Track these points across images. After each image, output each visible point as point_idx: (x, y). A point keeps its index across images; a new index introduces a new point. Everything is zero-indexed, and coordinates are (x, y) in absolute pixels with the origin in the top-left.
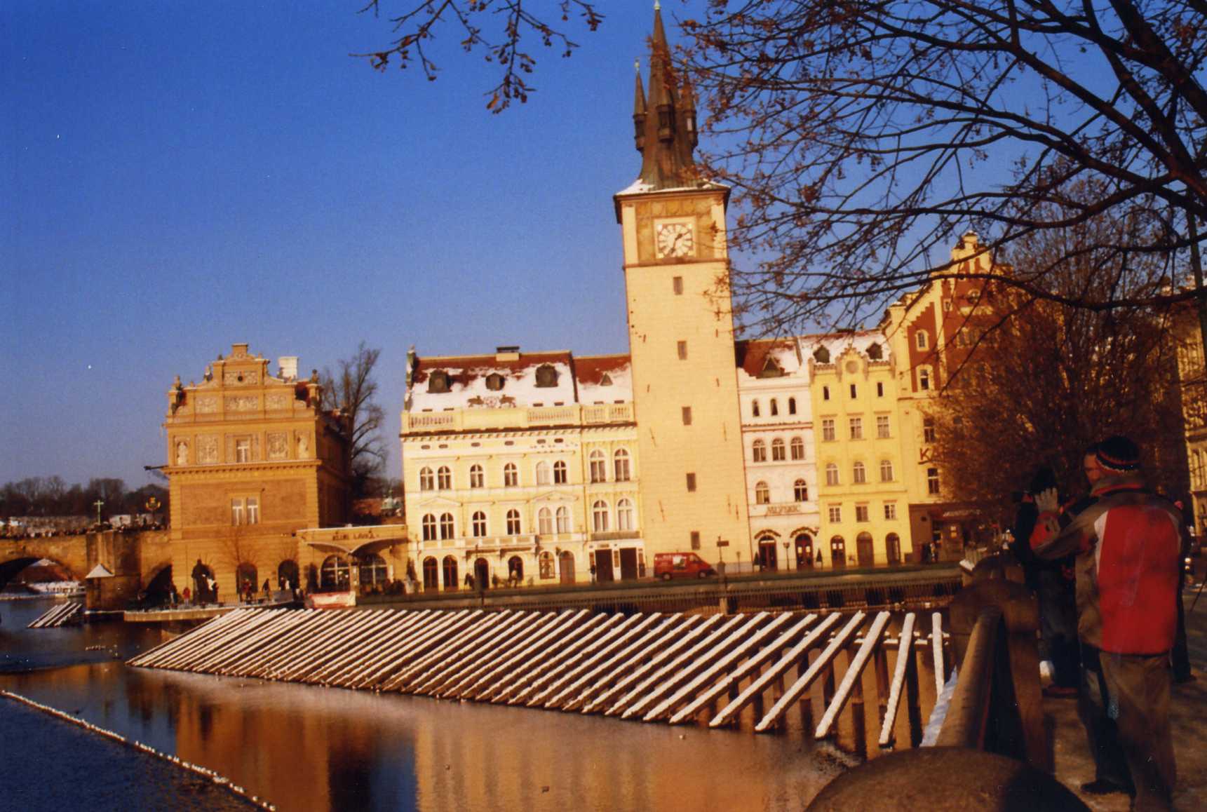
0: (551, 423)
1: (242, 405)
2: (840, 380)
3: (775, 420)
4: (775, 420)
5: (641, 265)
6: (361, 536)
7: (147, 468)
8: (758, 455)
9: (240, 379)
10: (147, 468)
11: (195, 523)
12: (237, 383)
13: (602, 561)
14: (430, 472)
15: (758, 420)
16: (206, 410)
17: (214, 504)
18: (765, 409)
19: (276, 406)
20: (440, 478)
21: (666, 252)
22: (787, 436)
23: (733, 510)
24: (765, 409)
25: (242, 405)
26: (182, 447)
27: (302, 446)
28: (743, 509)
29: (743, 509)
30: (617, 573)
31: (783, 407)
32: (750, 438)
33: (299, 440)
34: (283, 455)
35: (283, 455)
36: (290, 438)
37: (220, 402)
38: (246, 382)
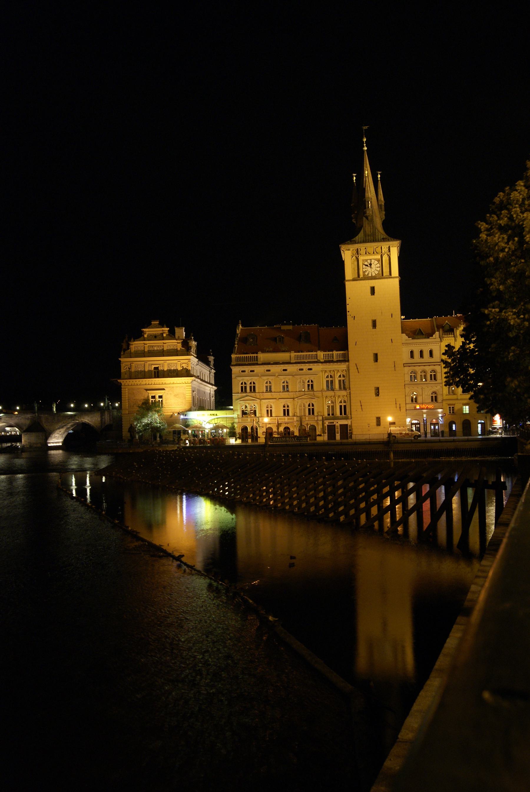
0: (306, 361)
2: (455, 340)
3: (422, 360)
4: (422, 360)
5: (354, 280)
8: (413, 377)
13: (331, 429)
14: (245, 383)
15: (412, 361)
18: (417, 355)
20: (251, 387)
21: (366, 274)
22: (428, 369)
23: (398, 406)
24: (417, 355)
28: (403, 405)
29: (403, 405)
30: (338, 437)
31: (426, 354)
32: (407, 370)
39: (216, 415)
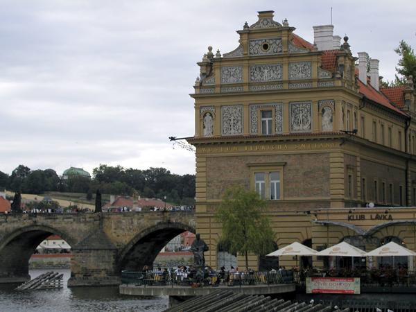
1: (267, 75)
6: (378, 218)
7: (172, 139)
9: (266, 47)
10: (172, 139)
11: (218, 197)
12: (262, 52)
16: (232, 80)
17: (236, 178)
19: (300, 76)
25: (267, 75)
26: (208, 117)
27: (326, 118)
33: (323, 111)
34: (306, 127)
35: (306, 127)
36: (314, 107)
37: (246, 71)
38: (270, 51)
39: (390, 218)
